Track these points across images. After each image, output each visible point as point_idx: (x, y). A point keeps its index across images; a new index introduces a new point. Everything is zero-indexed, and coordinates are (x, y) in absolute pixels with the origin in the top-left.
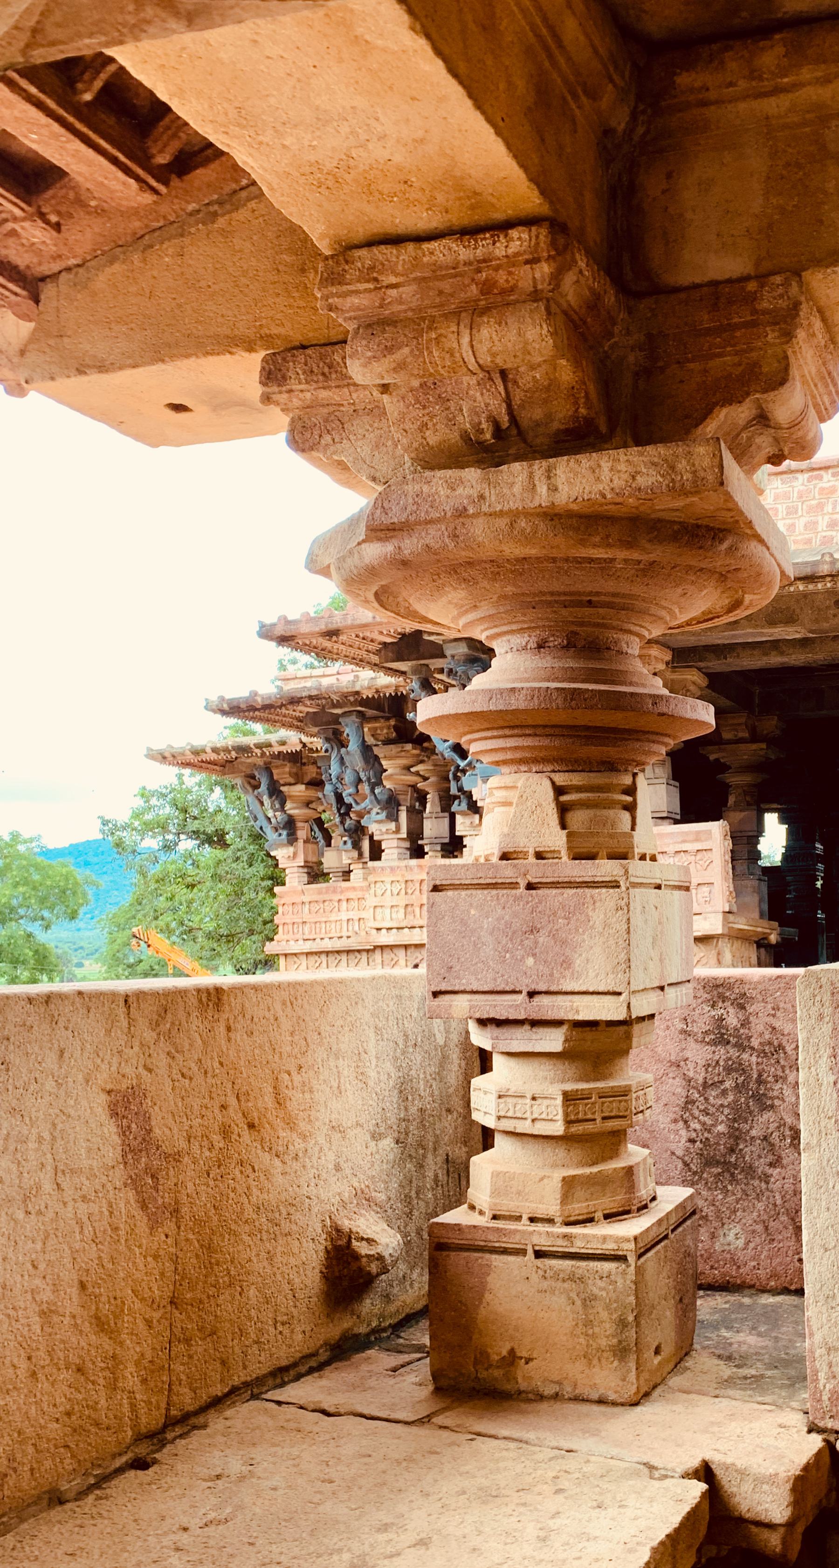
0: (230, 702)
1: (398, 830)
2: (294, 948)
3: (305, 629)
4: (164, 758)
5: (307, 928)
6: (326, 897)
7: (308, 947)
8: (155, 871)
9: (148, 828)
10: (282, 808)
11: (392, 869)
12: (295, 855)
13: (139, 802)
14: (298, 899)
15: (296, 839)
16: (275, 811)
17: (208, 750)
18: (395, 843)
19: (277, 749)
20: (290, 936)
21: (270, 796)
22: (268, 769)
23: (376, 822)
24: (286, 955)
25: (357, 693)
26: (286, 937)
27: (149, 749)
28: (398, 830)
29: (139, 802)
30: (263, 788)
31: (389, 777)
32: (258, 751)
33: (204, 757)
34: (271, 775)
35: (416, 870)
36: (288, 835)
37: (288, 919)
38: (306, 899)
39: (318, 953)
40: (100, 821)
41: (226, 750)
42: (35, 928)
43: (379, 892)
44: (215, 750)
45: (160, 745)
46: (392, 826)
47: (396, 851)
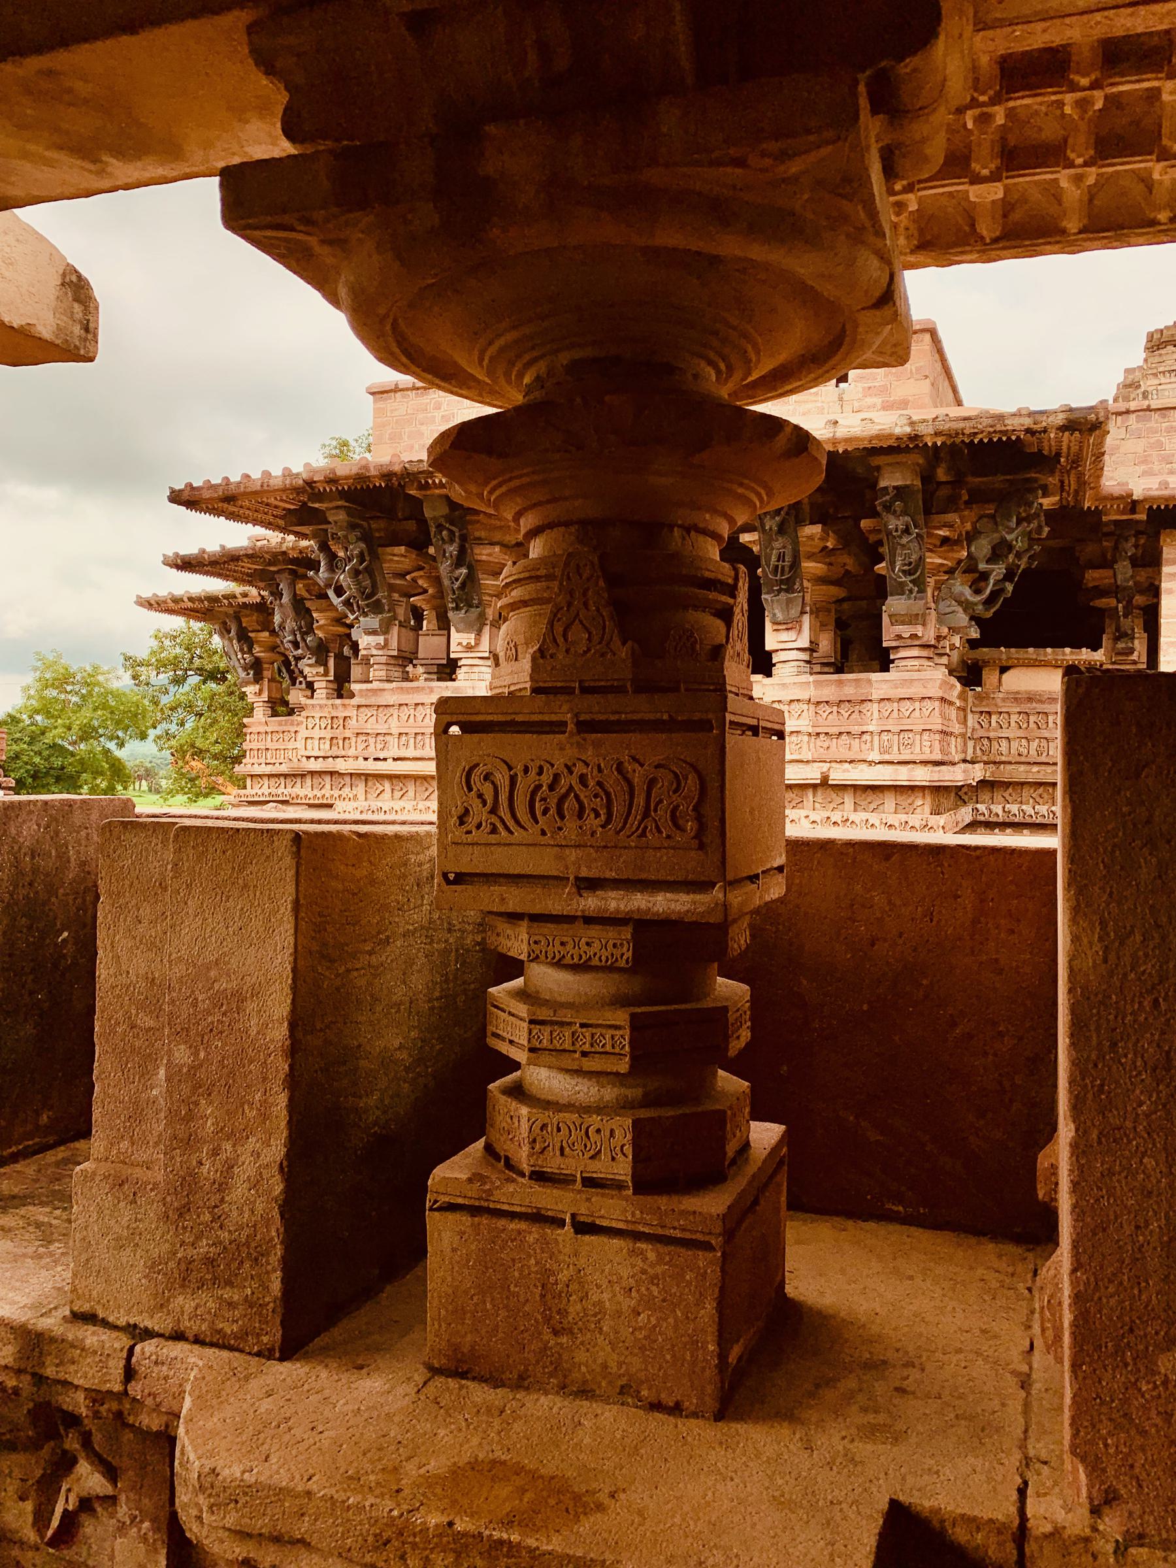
0: (183, 558)
1: (326, 674)
2: (258, 770)
3: (206, 495)
4: (151, 605)
5: (269, 754)
6: (285, 728)
7: (268, 770)
8: (165, 700)
9: (161, 666)
10: (250, 651)
11: (321, 706)
12: (261, 691)
13: (154, 644)
14: (262, 729)
15: (262, 679)
16: (243, 653)
17: (186, 599)
18: (324, 684)
19: (241, 600)
20: (255, 760)
21: (239, 641)
22: (237, 618)
23: (310, 665)
24: (252, 776)
25: (284, 553)
26: (252, 761)
27: (139, 597)
28: (326, 674)
29: (154, 644)
30: (233, 633)
31: (319, 628)
32: (226, 601)
33: (183, 605)
34: (240, 623)
35: (340, 708)
36: (254, 674)
37: (254, 745)
38: (269, 729)
39: (278, 776)
40: (122, 657)
41: (200, 600)
42: (112, 745)
43: (310, 726)
44: (191, 599)
45: (147, 594)
46: (321, 670)
47: (325, 691)
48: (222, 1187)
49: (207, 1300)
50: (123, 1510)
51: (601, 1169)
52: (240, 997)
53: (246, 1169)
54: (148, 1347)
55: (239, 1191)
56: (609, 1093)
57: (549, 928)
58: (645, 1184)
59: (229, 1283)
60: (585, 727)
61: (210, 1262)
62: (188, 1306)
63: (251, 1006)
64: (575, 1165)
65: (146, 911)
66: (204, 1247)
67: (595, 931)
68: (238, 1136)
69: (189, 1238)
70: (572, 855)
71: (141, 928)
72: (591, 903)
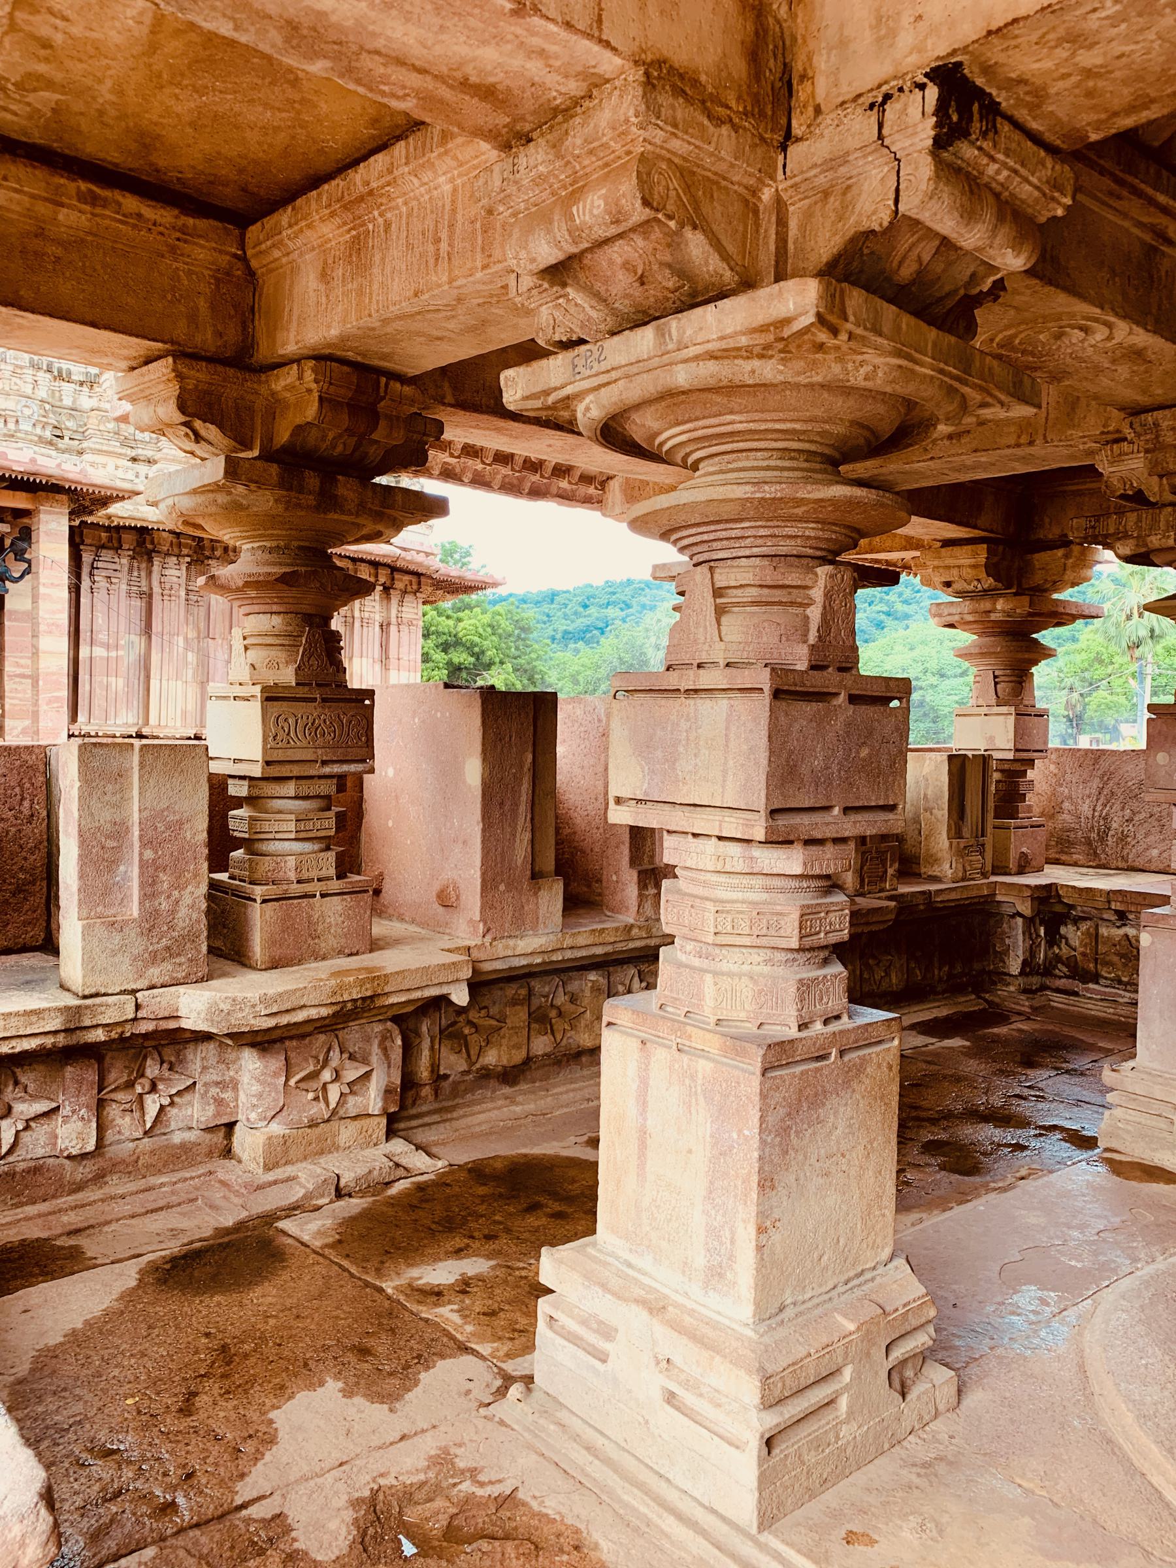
48: (173, 912)
49: (167, 966)
50: (66, 1111)
51: (324, 873)
52: (180, 823)
53: (187, 900)
54: (138, 995)
55: (183, 912)
56: (316, 847)
57: (303, 782)
58: (340, 876)
59: (179, 955)
60: (324, 700)
61: (168, 948)
62: (155, 973)
63: (186, 826)
64: (314, 874)
65: (109, 787)
66: (164, 942)
67: (322, 781)
68: (181, 888)
69: (155, 940)
70: (320, 752)
71: (107, 798)
72: (327, 770)
